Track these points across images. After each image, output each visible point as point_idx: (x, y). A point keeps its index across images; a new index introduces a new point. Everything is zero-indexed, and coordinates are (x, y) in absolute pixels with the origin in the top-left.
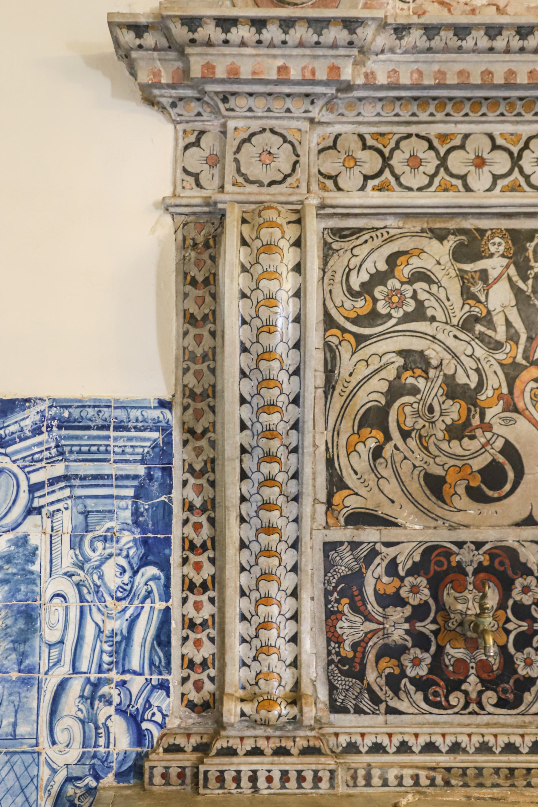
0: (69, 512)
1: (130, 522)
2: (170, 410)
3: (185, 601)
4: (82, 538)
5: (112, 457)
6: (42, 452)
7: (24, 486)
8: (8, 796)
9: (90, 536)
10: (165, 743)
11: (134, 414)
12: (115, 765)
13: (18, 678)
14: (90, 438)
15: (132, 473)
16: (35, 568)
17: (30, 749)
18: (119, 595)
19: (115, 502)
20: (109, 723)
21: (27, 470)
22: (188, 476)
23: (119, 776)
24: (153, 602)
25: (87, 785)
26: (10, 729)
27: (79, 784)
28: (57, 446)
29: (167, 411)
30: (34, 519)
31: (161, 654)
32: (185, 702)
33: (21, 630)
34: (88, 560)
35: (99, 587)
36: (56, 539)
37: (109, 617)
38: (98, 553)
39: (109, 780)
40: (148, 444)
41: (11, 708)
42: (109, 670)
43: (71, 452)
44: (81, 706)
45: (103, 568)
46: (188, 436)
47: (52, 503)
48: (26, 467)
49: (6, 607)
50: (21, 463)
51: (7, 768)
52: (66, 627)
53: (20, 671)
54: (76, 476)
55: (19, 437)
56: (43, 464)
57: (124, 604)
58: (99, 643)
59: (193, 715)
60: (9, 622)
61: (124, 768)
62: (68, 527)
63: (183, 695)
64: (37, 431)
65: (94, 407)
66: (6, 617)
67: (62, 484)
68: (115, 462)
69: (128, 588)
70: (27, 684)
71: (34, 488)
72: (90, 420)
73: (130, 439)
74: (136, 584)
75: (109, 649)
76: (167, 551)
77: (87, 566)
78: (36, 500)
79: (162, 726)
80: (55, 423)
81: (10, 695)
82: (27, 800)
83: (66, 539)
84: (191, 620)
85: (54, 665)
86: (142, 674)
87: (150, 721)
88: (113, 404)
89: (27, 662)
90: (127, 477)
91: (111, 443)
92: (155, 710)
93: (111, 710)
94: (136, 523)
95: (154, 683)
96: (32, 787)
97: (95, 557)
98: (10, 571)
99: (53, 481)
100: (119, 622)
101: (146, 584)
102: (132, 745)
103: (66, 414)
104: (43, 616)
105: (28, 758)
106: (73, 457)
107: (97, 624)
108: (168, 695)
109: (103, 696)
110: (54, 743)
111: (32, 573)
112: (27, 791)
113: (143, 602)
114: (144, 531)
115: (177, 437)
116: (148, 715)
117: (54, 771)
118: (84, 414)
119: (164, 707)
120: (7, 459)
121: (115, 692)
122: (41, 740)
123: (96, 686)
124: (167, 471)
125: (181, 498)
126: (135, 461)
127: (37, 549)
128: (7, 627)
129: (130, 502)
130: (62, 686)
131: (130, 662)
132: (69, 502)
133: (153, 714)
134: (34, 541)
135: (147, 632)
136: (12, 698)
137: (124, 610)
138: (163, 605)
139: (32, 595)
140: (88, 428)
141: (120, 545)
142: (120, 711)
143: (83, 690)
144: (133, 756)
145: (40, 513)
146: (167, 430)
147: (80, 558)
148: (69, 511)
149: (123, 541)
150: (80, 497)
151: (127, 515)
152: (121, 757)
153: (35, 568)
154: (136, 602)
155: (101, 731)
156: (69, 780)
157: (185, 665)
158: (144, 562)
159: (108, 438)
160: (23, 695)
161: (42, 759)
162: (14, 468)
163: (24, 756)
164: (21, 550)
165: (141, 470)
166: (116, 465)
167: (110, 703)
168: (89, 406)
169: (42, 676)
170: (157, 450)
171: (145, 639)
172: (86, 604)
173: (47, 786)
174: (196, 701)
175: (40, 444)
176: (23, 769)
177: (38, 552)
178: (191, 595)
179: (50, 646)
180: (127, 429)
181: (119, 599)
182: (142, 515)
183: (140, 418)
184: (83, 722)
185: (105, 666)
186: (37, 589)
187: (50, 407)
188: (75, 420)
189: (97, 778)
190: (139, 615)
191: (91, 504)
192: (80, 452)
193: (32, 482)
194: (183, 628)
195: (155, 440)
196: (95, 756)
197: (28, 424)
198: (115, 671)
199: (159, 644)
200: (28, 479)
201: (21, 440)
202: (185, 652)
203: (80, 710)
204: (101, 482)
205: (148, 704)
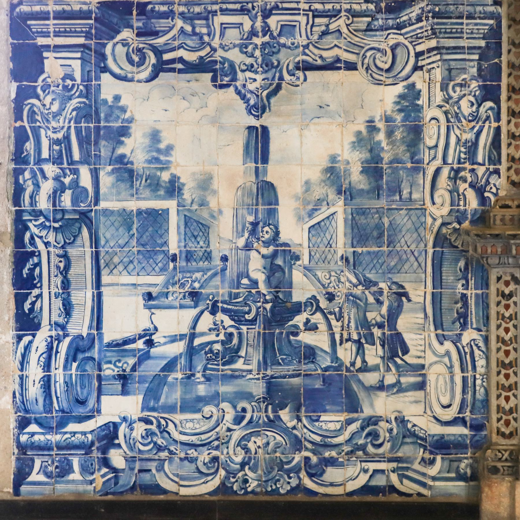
0: (439, 69)
1: (476, 75)
2: (501, 6)
3: (509, 122)
4: (448, 85)
5: (465, 36)
6: (422, 32)
7: (412, 53)
8: (408, 233)
9: (452, 83)
10: (500, 203)
11: (479, 9)
12: (469, 216)
13: (412, 167)
14: (452, 24)
15: (477, 45)
16: (420, 102)
17: (420, 207)
18: (470, 118)
19: (467, 63)
20: (465, 193)
21: (414, 43)
22: (511, 47)
23: (472, 222)
24: (490, 123)
25: (454, 227)
26: (408, 196)
27: (449, 227)
28: (432, 29)
29: (499, 7)
30: (418, 73)
31: (495, 153)
32: (510, 181)
33: (412, 140)
34: (451, 98)
35: (458, 114)
36: (432, 85)
37: (465, 131)
38: (457, 94)
39: (466, 224)
40: (487, 27)
41: (408, 184)
42: (464, 163)
43: (440, 33)
44: (449, 183)
45: (460, 102)
46: (512, 23)
47: (430, 64)
48: (413, 42)
49: (403, 125)
50: (410, 40)
51: (406, 218)
52: (439, 138)
53: (412, 163)
54: (443, 48)
55: (409, 24)
56: (423, 40)
57: (473, 124)
58: (458, 147)
59: (515, 189)
60: (405, 134)
61: (476, 218)
62: (439, 78)
63: (508, 177)
64: (419, 19)
65: (454, 5)
66: (403, 132)
67: (435, 52)
68: (467, 38)
69: (475, 114)
70: (417, 170)
71: (418, 55)
72: (452, 13)
73: (476, 24)
74: (480, 112)
75: (464, 150)
76: (498, 93)
77: (450, 101)
78: (420, 62)
79: (496, 195)
80: (430, 15)
81: (407, 176)
82: (419, 235)
83: (438, 85)
84: (513, 133)
85: (433, 159)
86: (484, 165)
87: (489, 192)
88: (465, 3)
89: (416, 158)
90: (474, 48)
91: (465, 27)
92: (492, 186)
93: (466, 185)
94: (480, 75)
95: (491, 170)
96: (422, 228)
97: (455, 96)
98: (405, 104)
99: (430, 50)
100: (470, 134)
101: (486, 112)
102: (479, 205)
103: (437, 9)
104: (425, 131)
105: (419, 212)
106: (441, 36)
107: (457, 136)
108: (499, 177)
109: (461, 178)
110: (434, 203)
111: (418, 105)
112: (419, 231)
113: (484, 122)
114: (484, 81)
115: (504, 23)
116: (488, 188)
117: (435, 219)
118: (447, 9)
119: (497, 184)
120: (402, 37)
121: (468, 175)
122: (426, 202)
123: (457, 171)
124: (499, 45)
125: (506, 60)
126: (479, 38)
127: (420, 91)
128: (404, 137)
129: (476, 63)
130: (437, 172)
131: (477, 158)
132: (440, 63)
133: (491, 188)
134: (419, 86)
135: (487, 140)
136: (409, 178)
137: (473, 127)
138: (496, 125)
139: (419, 119)
140: (450, 18)
141: (470, 89)
142: (472, 186)
143: (450, 174)
144: (480, 212)
145: (422, 70)
146: (498, 18)
147: (447, 97)
148: (439, 69)
149: (472, 86)
150: (446, 60)
151: (474, 71)
152: (473, 212)
153: (420, 102)
154: (480, 123)
155: (461, 197)
156: (443, 224)
157: (510, 159)
158: (485, 99)
159: (462, 24)
160: (415, 176)
161: (427, 213)
162: (406, 43)
163: (417, 211)
164: (411, 92)
165: (483, 43)
166: (467, 41)
167: (465, 181)
168: (451, 4)
169: (425, 166)
170: (492, 31)
171: (485, 144)
172: (450, 124)
173: (430, 228)
174: (516, 181)
175: (421, 28)
176: (416, 218)
177: (422, 93)
178: (513, 119)
179: (430, 148)
180: (474, 18)
181: (470, 121)
182: (483, 70)
183: (482, 11)
184: (450, 192)
185: (462, 160)
186: (421, 115)
187: (427, 5)
188: (443, 13)
189: (460, 223)
190: (482, 131)
191: (453, 64)
192: (445, 33)
193: (417, 51)
194: (508, 138)
195: (491, 25)
196: (458, 211)
197: (414, 15)
198: (468, 163)
199: (494, 148)
200: (415, 49)
201: (410, 25)
202: (510, 152)
203: (448, 185)
204: (459, 51)
205: (488, 182)
